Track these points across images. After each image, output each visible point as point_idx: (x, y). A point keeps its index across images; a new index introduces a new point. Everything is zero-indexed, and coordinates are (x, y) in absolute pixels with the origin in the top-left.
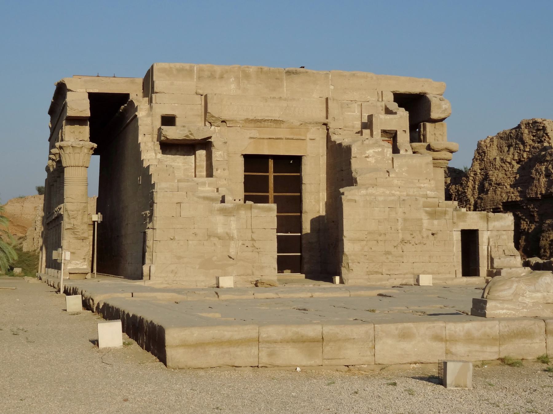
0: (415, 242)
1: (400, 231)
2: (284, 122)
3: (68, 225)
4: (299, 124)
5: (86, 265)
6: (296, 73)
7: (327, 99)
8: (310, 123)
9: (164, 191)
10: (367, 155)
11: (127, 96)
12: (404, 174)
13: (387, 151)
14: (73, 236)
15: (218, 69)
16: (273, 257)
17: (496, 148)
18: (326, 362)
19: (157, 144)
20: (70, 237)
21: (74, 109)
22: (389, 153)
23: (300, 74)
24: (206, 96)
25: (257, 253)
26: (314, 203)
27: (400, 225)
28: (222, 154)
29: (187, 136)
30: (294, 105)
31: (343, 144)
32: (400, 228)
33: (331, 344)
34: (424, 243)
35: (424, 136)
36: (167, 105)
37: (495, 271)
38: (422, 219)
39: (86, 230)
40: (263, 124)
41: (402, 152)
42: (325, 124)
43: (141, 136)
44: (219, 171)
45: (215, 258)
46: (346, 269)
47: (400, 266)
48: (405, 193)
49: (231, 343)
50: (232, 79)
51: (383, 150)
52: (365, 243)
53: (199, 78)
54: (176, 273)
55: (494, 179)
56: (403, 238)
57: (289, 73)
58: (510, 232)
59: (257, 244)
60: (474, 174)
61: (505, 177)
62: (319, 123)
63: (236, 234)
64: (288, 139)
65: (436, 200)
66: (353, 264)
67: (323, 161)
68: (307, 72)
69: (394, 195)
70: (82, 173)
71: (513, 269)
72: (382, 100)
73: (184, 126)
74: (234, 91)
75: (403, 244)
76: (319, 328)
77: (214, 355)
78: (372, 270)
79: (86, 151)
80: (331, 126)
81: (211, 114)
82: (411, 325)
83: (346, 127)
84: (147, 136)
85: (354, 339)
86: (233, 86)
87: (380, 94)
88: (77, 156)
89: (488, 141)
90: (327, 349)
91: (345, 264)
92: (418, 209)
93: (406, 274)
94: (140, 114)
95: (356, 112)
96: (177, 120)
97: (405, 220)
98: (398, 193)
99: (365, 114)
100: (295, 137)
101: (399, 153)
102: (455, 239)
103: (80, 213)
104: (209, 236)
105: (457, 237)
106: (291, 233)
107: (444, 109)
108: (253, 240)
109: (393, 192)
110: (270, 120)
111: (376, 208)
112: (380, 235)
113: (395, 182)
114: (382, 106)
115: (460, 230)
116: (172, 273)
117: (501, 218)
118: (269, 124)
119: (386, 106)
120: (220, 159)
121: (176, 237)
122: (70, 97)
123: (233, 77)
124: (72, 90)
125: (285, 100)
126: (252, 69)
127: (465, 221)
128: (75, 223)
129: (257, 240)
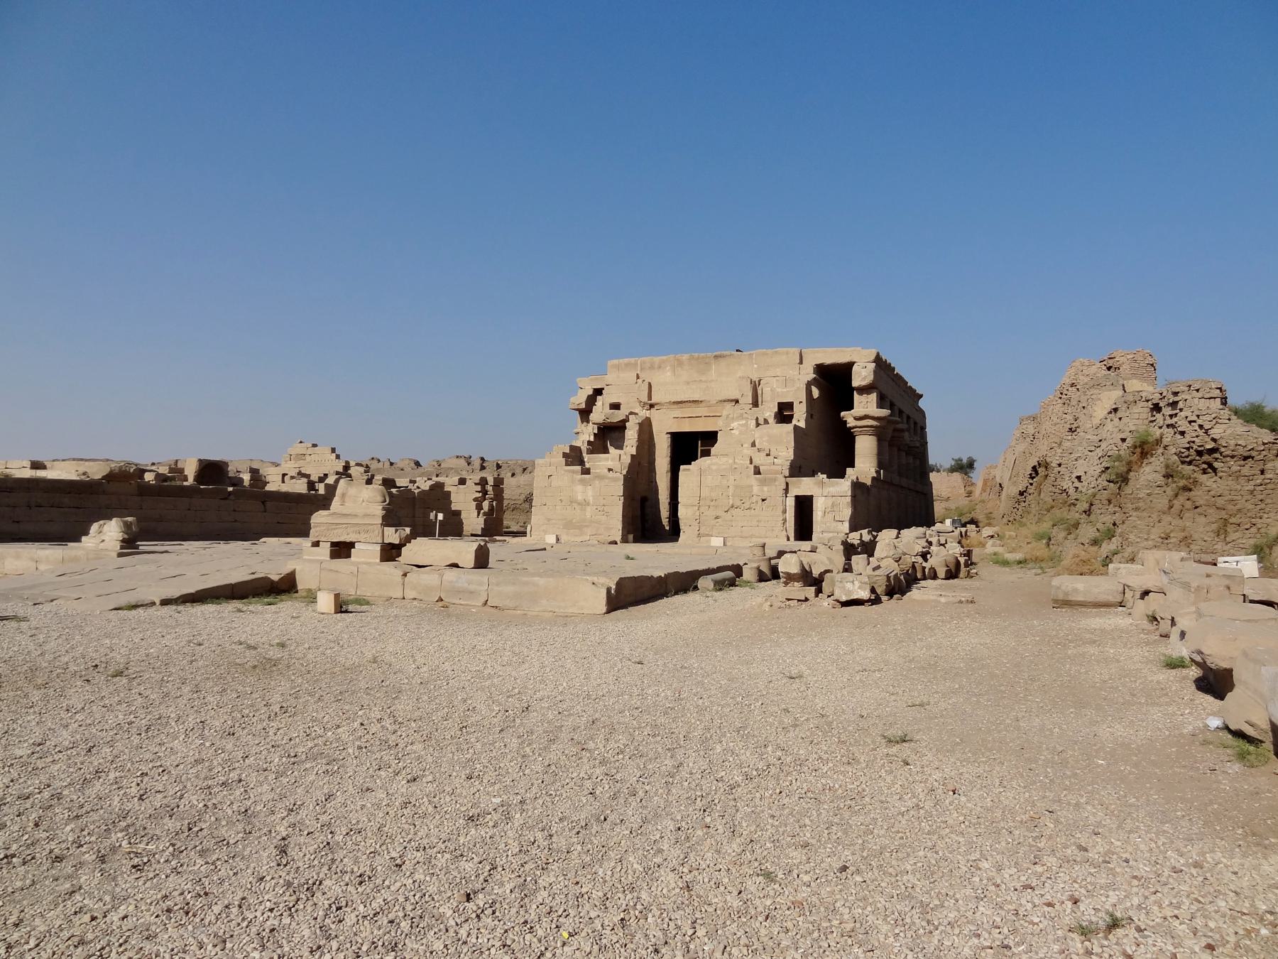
4: (715, 402)
8: (725, 401)
10: (731, 428)
15: (657, 359)
29: (604, 420)
38: (752, 486)
45: (574, 521)
53: (641, 369)
86: (669, 374)
93: (735, 537)
96: (621, 406)
97: (736, 487)
100: (712, 415)
104: (571, 502)
117: (837, 483)
125: (706, 382)
126: (685, 357)
127: (799, 487)
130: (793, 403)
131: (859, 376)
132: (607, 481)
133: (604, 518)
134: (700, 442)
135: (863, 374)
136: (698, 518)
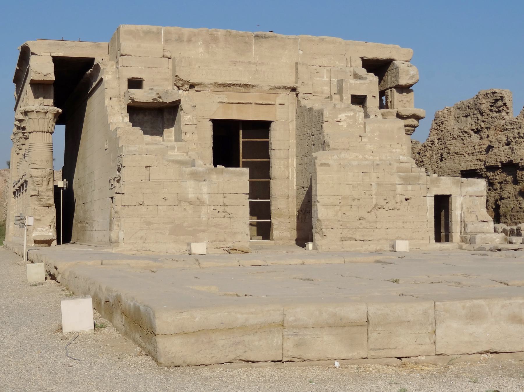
0: (389, 208)
1: (374, 196)
2: (253, 86)
3: (33, 191)
4: (268, 88)
5: (52, 232)
6: (265, 37)
7: (297, 63)
8: (280, 88)
9: (132, 154)
10: (339, 119)
11: (93, 60)
12: (376, 138)
13: (359, 116)
14: (38, 203)
16: (245, 223)
17: (454, 118)
18: (373, 353)
19: (124, 107)
20: (35, 204)
21: (38, 72)
22: (361, 117)
23: (268, 39)
24: (174, 59)
25: (229, 218)
26: (283, 169)
27: (374, 190)
28: (191, 118)
29: (155, 99)
30: (263, 70)
31: (314, 109)
32: (373, 193)
33: (380, 329)
34: (398, 209)
35: (391, 102)
36: (134, 68)
37: (468, 237)
38: (396, 184)
39: (51, 196)
40: (231, 89)
41: (372, 117)
42: (294, 90)
43: (107, 99)
44: (188, 135)
45: (185, 224)
46: (319, 235)
47: (373, 232)
48: (378, 158)
49: (245, 329)
50: (200, 43)
51: (355, 114)
52: (338, 208)
53: (167, 41)
54: (145, 239)
55: (452, 148)
56: (377, 203)
57: (258, 37)
58: (483, 197)
59: (228, 209)
60: (432, 144)
61: (463, 146)
62: (289, 88)
63: (207, 199)
64: (257, 104)
65: (409, 166)
66: (327, 230)
67: (293, 126)
68: (276, 37)
69: (366, 159)
70: (47, 139)
71: (488, 235)
72: (351, 66)
73: (152, 89)
74: (202, 54)
75: (377, 210)
76: (363, 308)
77: (223, 346)
78: (345, 236)
79: (51, 116)
80: (299, 90)
81: (179, 78)
82: (482, 302)
83: (315, 92)
84: (113, 99)
85: (408, 321)
86: (201, 50)
87: (349, 60)
88: (41, 121)
89: (446, 112)
90: (374, 335)
91: (318, 230)
92: (392, 174)
93: (380, 240)
94: (107, 78)
95: (325, 77)
96: (144, 83)
97: (379, 185)
98: (371, 158)
99: (334, 80)
100: (264, 102)
101: (369, 118)
102: (428, 204)
103: (45, 179)
104: (180, 201)
105: (431, 202)
106: (260, 199)
107: (412, 75)
108: (225, 205)
109: (367, 156)
110: (239, 84)
111: (350, 173)
112: (354, 200)
113: (368, 146)
114: (351, 72)
115: (434, 196)
116: (141, 239)
117: (474, 183)
118: (238, 88)
119: (354, 72)
120: (189, 123)
121: (145, 202)
122: (33, 61)
123: (201, 41)
124: (36, 53)
125: (255, 64)
127: (438, 187)
128: (40, 190)
129: (229, 205)
130: (366, 96)
131: (407, 75)
132: (228, 175)
133: (226, 220)
134: (241, 131)
135: (412, 73)
136: (340, 219)
